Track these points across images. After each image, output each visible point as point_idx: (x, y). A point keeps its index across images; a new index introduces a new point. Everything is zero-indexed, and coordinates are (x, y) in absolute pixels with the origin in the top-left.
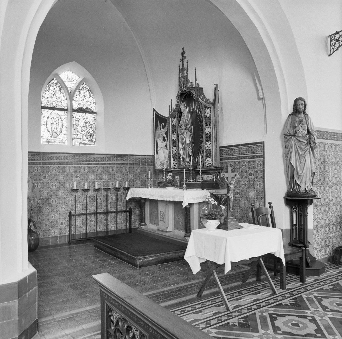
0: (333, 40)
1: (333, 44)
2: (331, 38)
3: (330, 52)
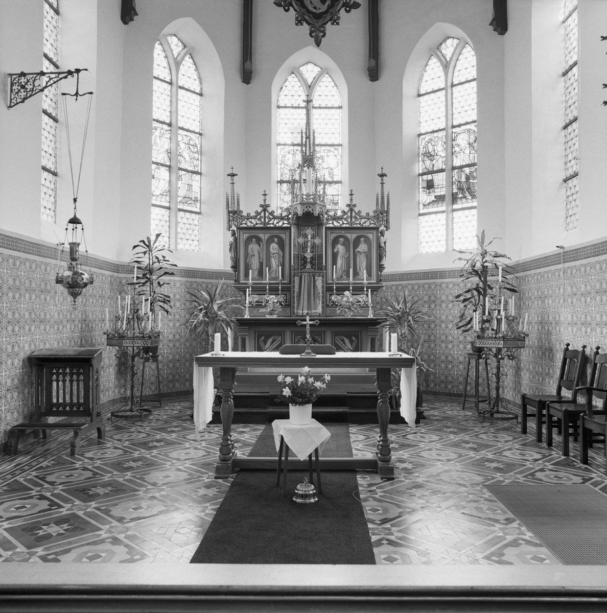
0: (16, 83)
1: (17, 91)
2: (13, 79)
3: (11, 102)
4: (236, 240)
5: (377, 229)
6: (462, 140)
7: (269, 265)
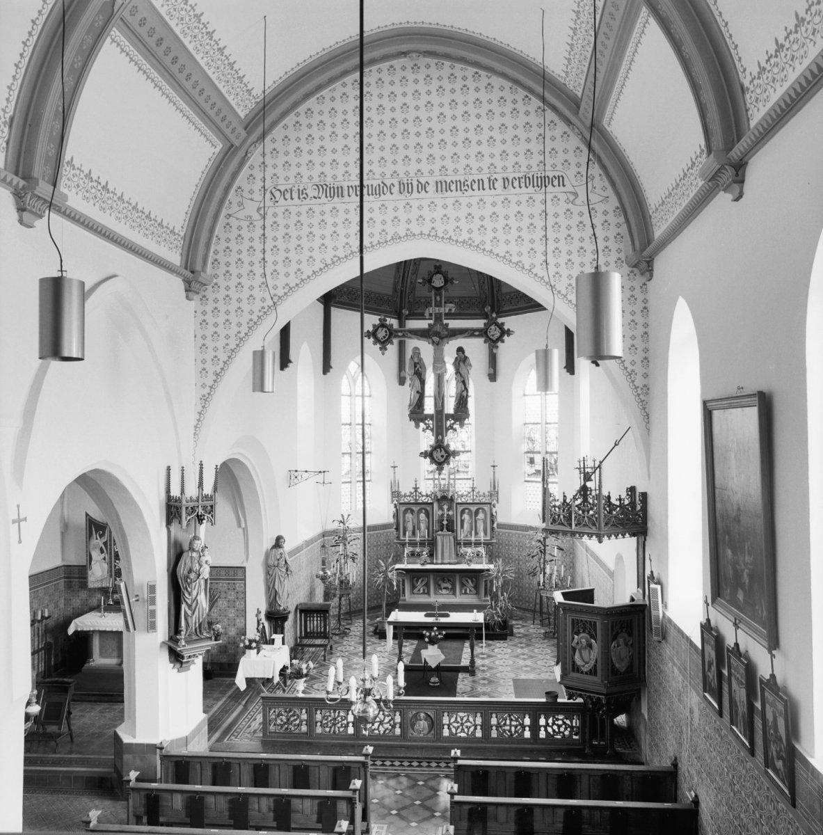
4: (397, 510)
5: (490, 504)
6: (553, 434)
7: (419, 529)
